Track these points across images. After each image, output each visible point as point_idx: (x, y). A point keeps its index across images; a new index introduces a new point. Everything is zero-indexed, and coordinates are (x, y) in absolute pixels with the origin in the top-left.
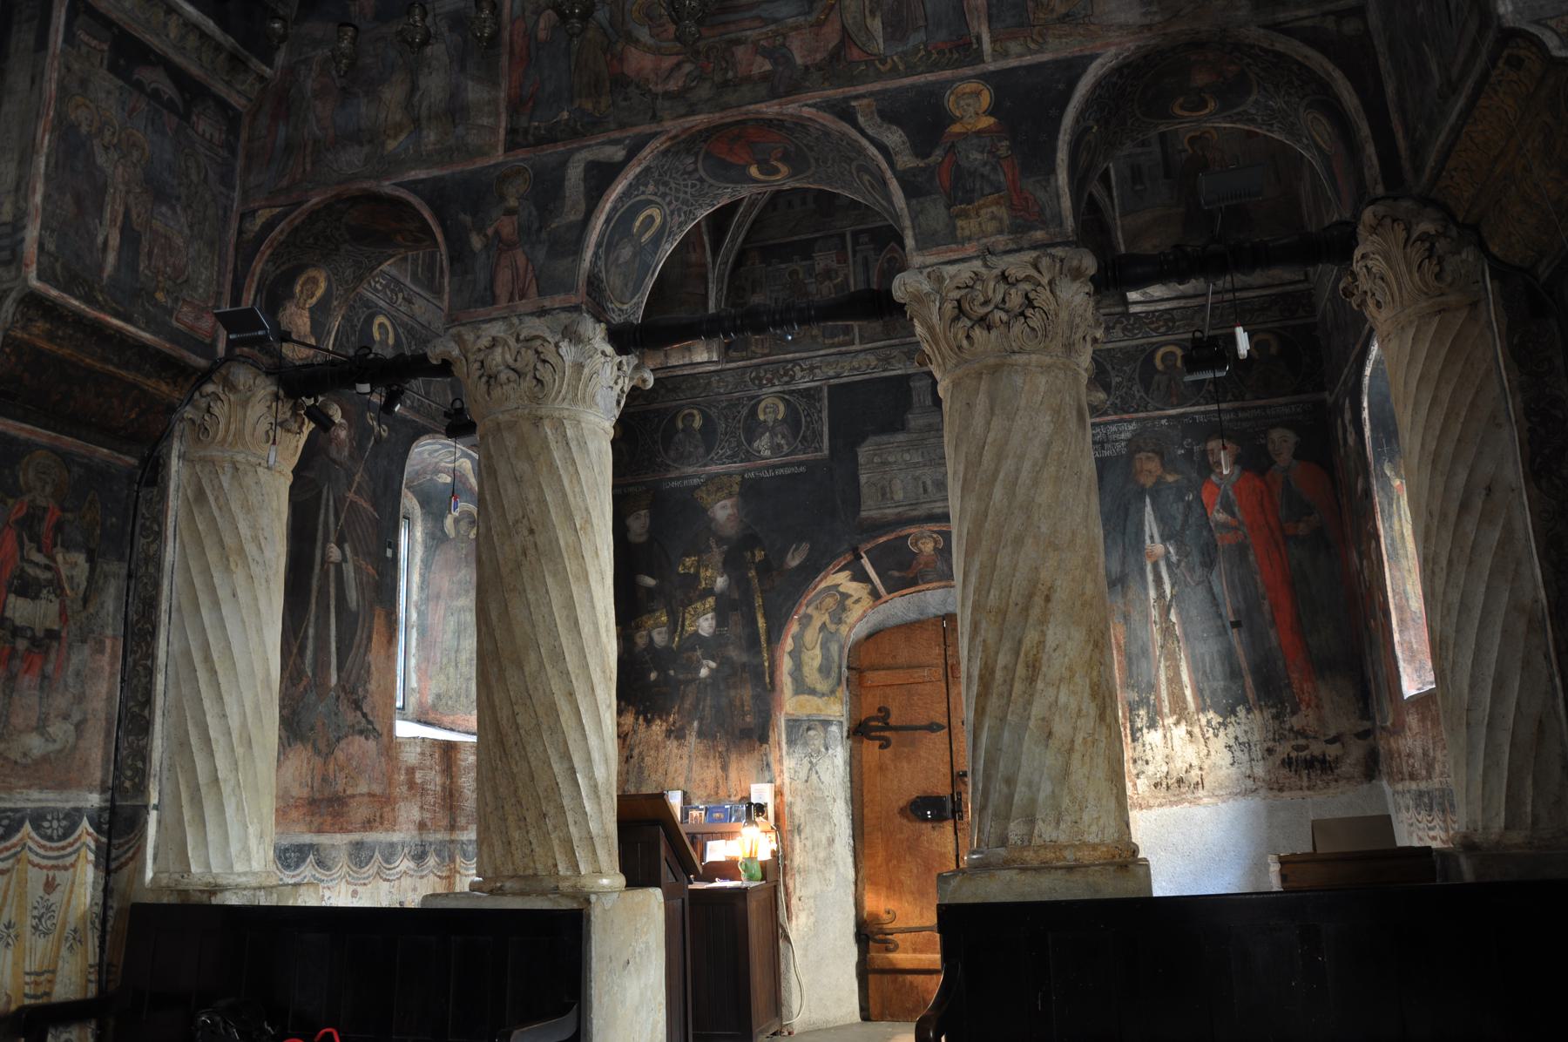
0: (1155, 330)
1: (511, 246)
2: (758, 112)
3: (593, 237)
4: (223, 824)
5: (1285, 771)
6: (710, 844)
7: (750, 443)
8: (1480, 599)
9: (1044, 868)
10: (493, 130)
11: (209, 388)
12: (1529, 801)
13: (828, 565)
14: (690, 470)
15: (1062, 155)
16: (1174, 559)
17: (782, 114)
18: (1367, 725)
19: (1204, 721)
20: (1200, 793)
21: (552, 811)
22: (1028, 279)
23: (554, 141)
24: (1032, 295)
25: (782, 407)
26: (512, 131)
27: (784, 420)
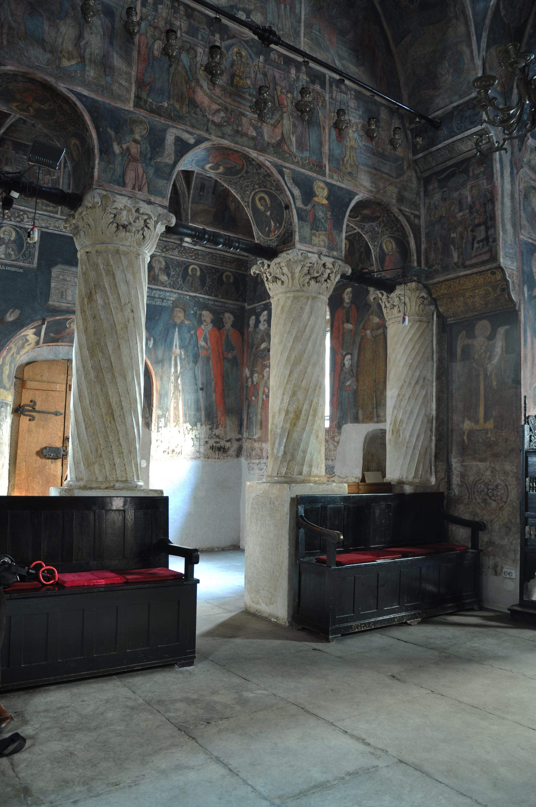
0: (191, 256)
1: (135, 160)
2: (248, 152)
5: (210, 451)
8: (416, 411)
10: (128, 91)
12: (421, 471)
13: (29, 324)
16: (183, 357)
17: (257, 158)
18: (240, 436)
19: (185, 428)
20: (180, 456)
21: (133, 450)
22: (330, 269)
23: (160, 115)
24: (331, 275)
25: (14, 234)
27: (14, 241)
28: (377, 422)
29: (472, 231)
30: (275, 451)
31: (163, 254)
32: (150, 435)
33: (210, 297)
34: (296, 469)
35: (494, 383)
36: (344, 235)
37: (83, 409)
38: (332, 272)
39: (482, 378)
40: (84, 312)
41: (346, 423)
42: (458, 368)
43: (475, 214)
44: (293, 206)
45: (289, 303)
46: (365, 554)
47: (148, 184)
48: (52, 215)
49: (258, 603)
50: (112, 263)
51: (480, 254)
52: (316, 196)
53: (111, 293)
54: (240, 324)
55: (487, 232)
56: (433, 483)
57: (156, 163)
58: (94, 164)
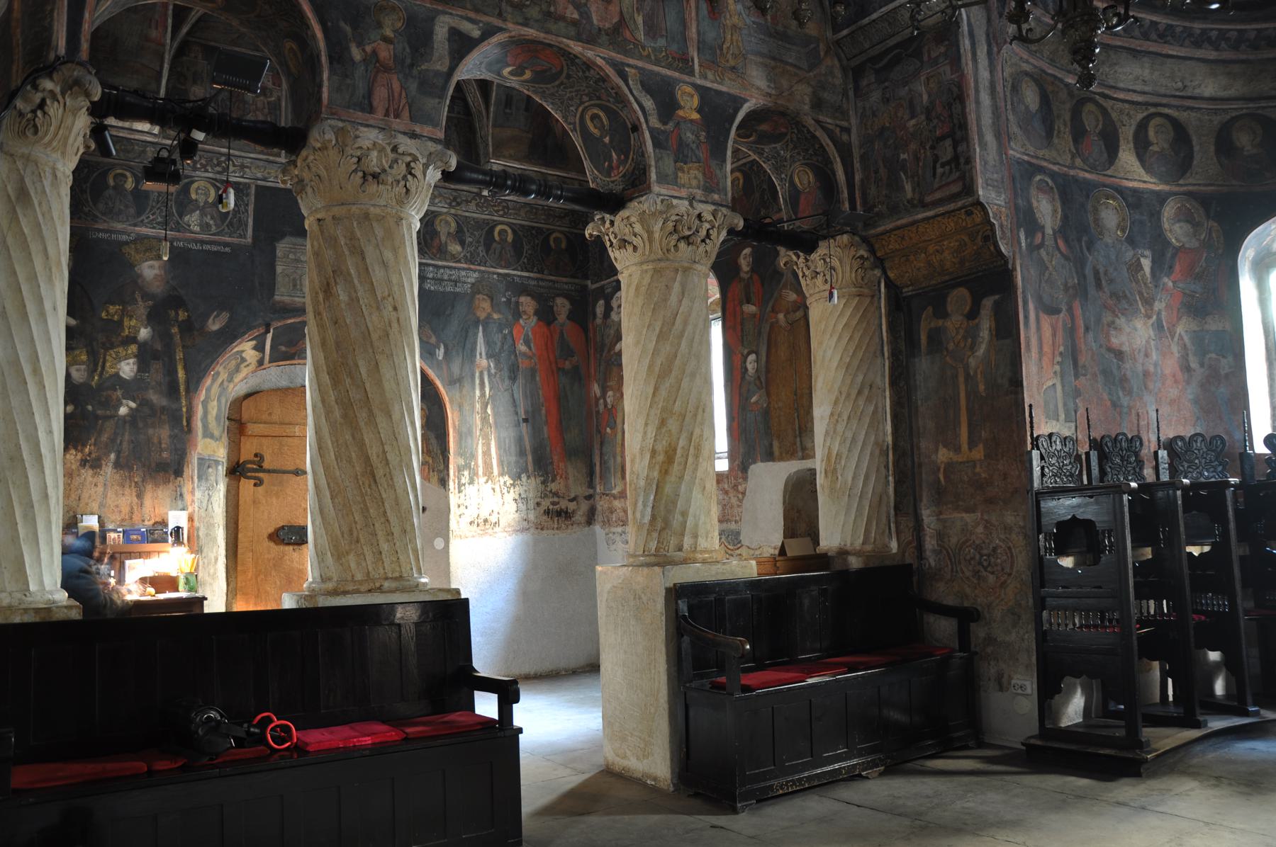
1: (387, 70)
5: (545, 518)
6: (128, 562)
7: (181, 215)
8: (862, 437)
11: (48, 85)
13: (245, 333)
14: (119, 226)
16: (493, 371)
18: (591, 491)
20: (497, 529)
21: (408, 528)
28: (803, 458)
29: (933, 148)
30: (638, 515)
31: (453, 211)
32: (447, 498)
33: (532, 275)
34: (673, 542)
35: (982, 387)
36: (729, 167)
37: (327, 468)
38: (713, 227)
39: (961, 379)
40: (319, 314)
41: (755, 462)
42: (924, 366)
43: (935, 121)
44: (644, 126)
45: (647, 280)
46: (788, 671)
47: (410, 107)
48: (271, 158)
49: (625, 757)
50: (358, 234)
51: (948, 184)
52: (680, 107)
53: (360, 282)
54: (582, 312)
55: (955, 148)
56: (895, 551)
57: (420, 73)
58: (321, 81)
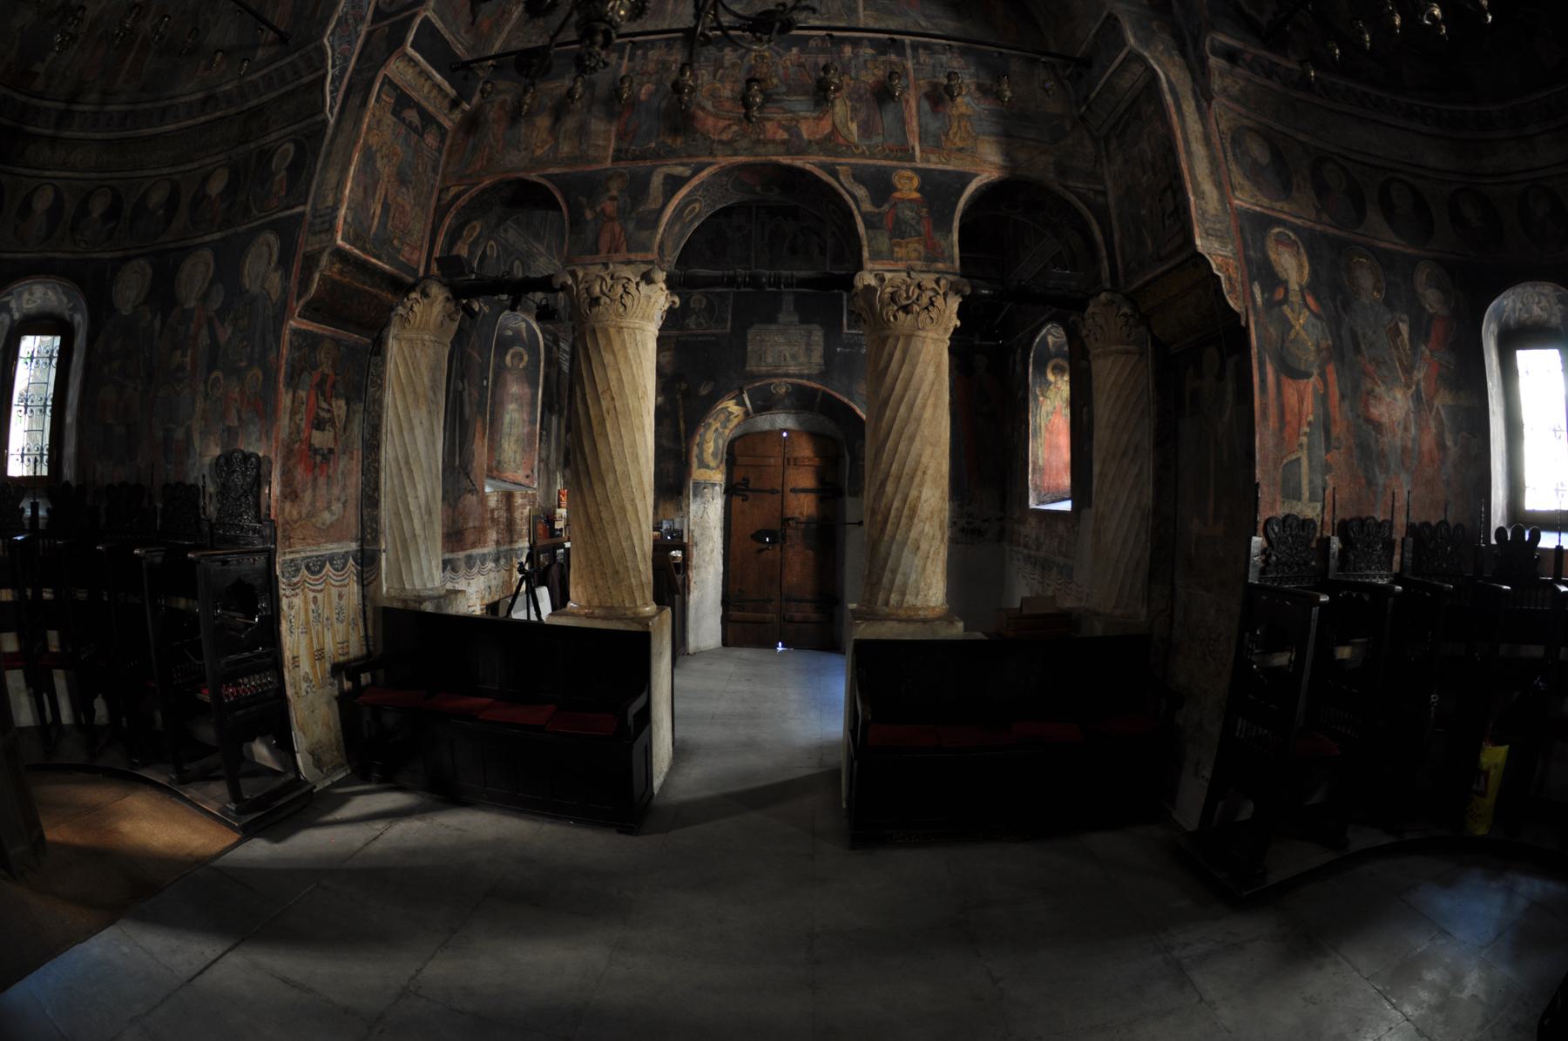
1: (611, 219)
3: (665, 219)
4: (419, 562)
9: (909, 620)
10: (606, 148)
11: (413, 295)
15: (956, 224)
21: (621, 570)
23: (645, 159)
26: (618, 151)
44: (856, 212)
52: (896, 190)
